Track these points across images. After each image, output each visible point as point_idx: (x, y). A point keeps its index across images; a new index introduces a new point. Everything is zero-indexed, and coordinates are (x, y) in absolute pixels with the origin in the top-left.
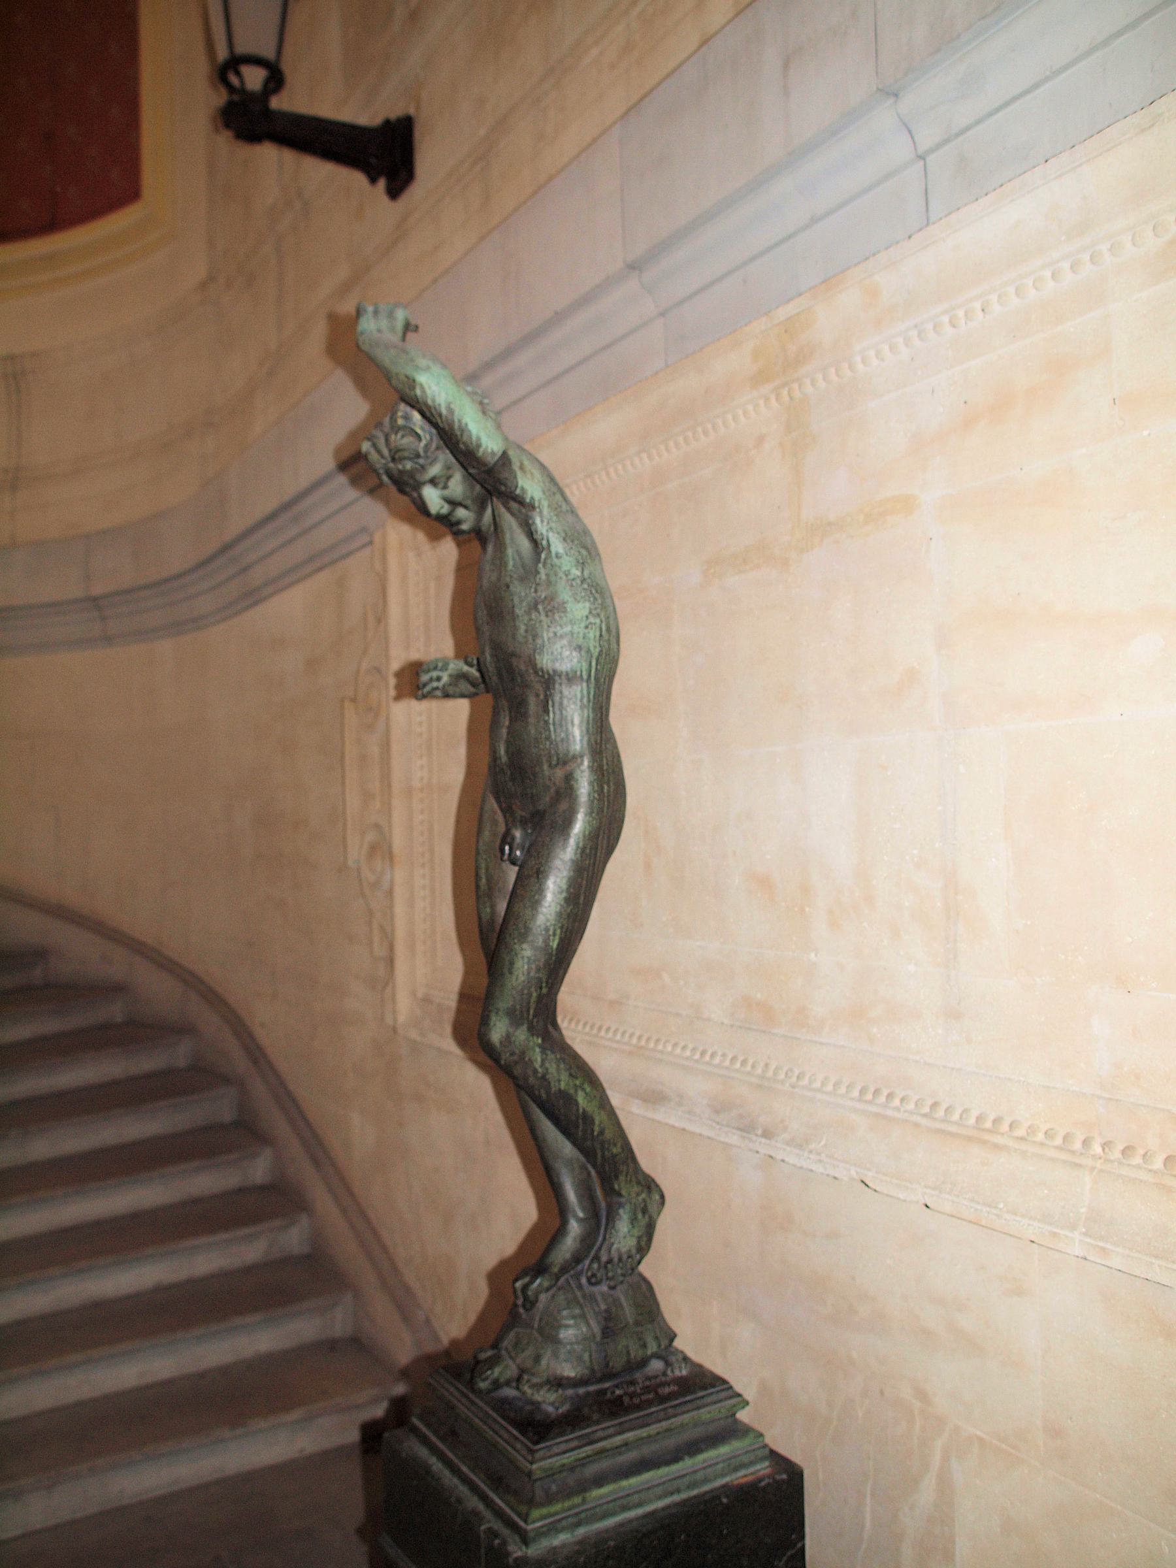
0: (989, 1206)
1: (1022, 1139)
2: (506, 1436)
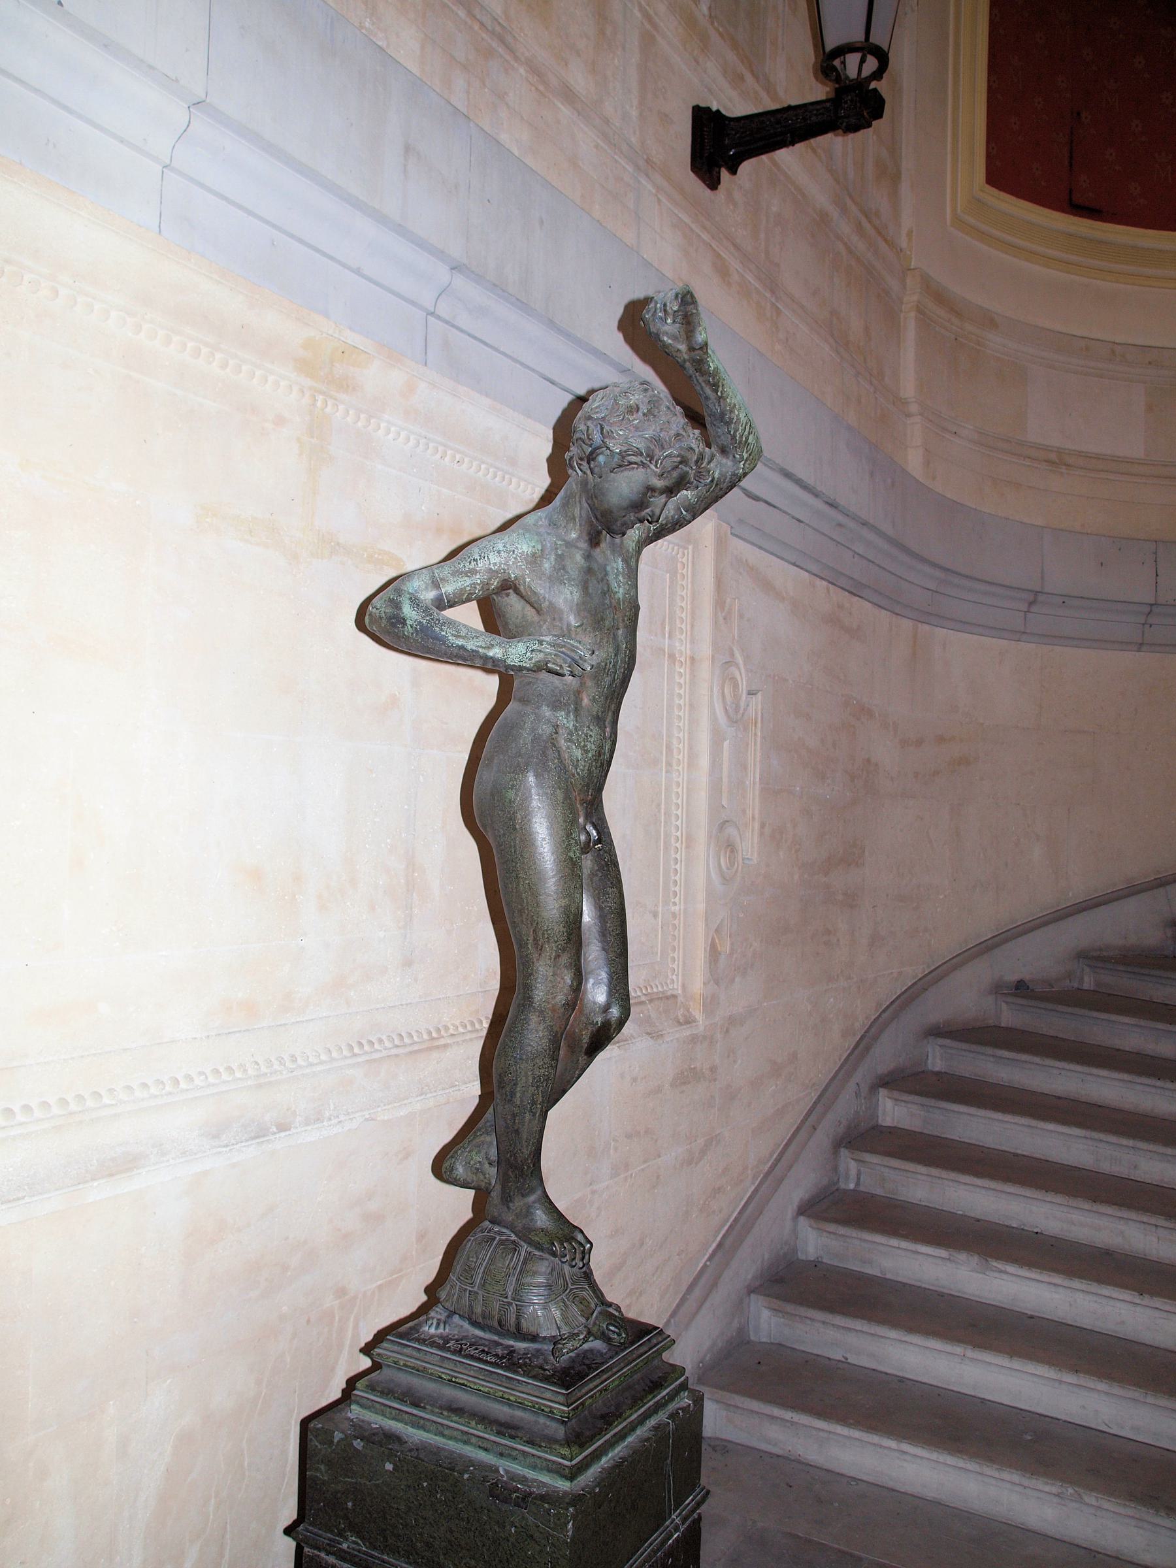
2: (645, 1348)
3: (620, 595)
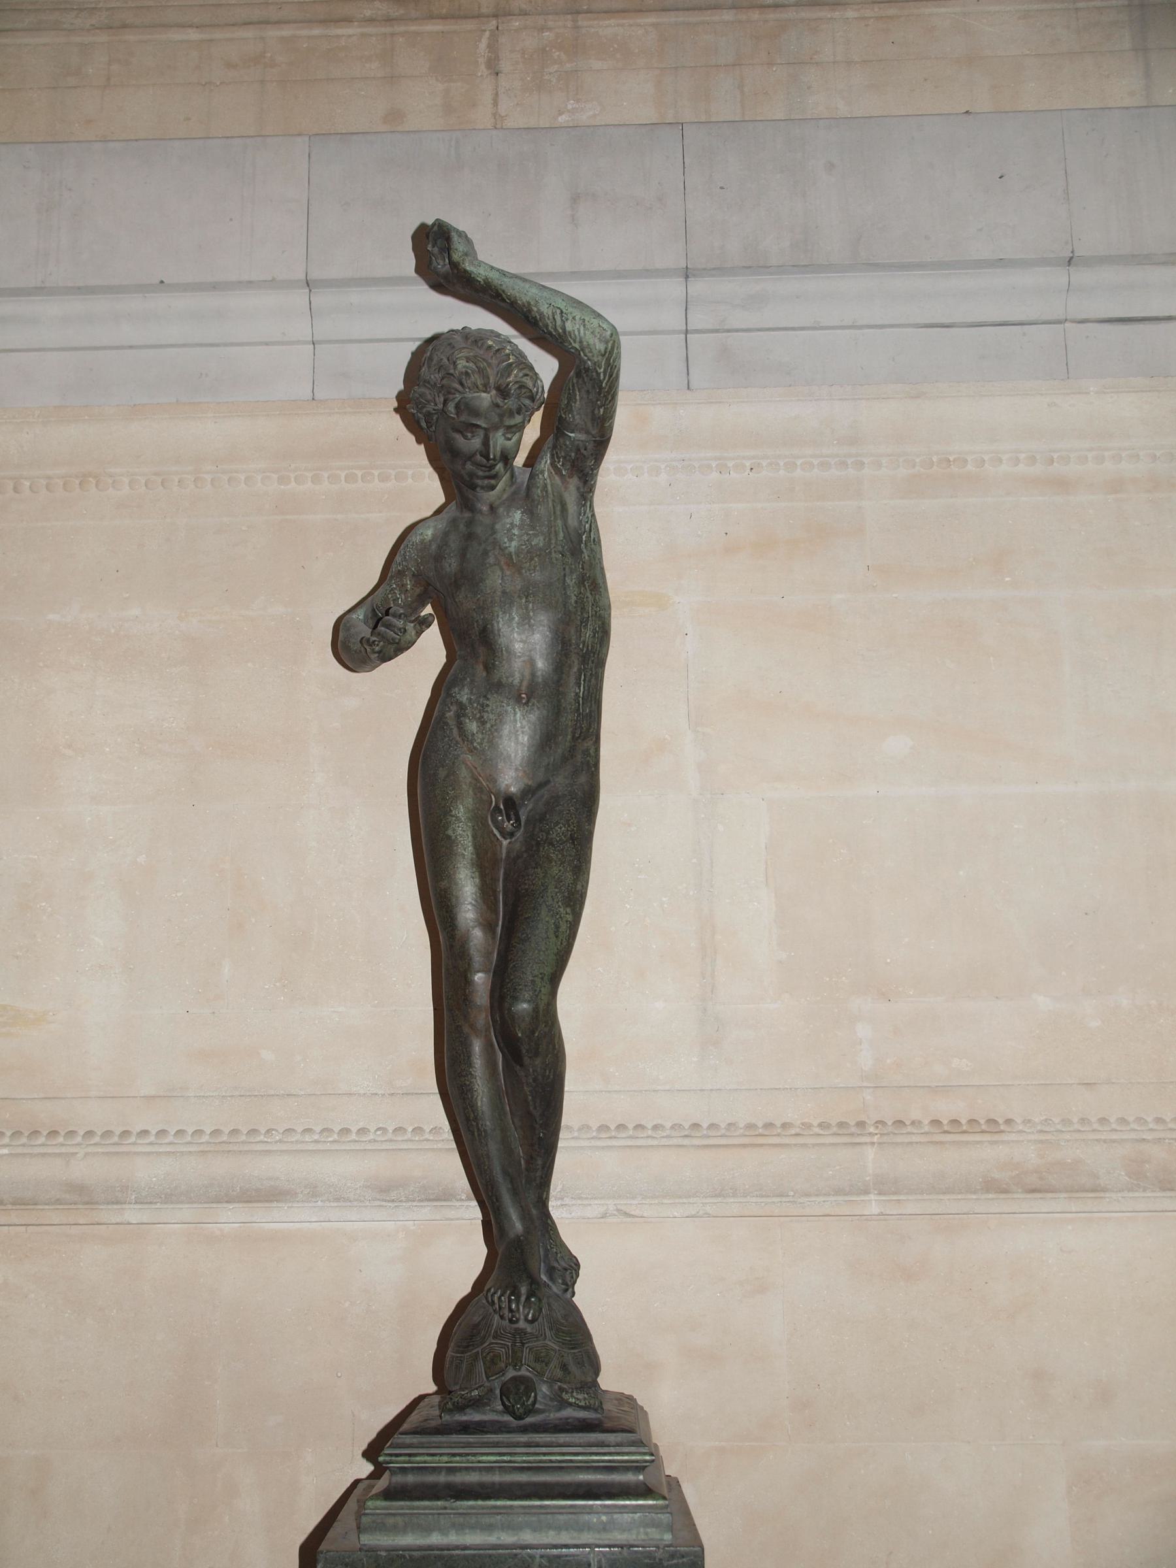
0: (781, 1196)
1: (797, 1135)
3: (512, 549)
